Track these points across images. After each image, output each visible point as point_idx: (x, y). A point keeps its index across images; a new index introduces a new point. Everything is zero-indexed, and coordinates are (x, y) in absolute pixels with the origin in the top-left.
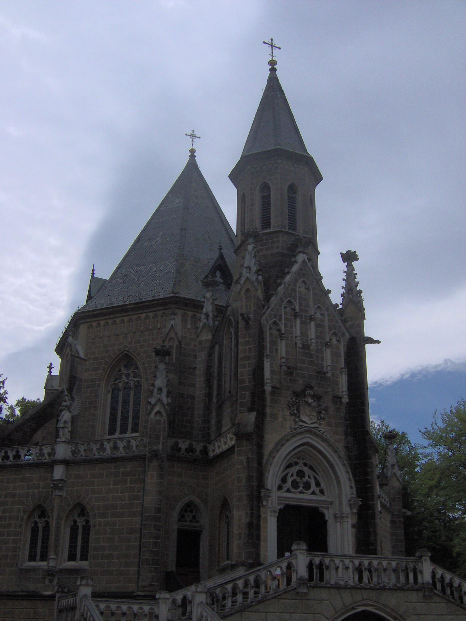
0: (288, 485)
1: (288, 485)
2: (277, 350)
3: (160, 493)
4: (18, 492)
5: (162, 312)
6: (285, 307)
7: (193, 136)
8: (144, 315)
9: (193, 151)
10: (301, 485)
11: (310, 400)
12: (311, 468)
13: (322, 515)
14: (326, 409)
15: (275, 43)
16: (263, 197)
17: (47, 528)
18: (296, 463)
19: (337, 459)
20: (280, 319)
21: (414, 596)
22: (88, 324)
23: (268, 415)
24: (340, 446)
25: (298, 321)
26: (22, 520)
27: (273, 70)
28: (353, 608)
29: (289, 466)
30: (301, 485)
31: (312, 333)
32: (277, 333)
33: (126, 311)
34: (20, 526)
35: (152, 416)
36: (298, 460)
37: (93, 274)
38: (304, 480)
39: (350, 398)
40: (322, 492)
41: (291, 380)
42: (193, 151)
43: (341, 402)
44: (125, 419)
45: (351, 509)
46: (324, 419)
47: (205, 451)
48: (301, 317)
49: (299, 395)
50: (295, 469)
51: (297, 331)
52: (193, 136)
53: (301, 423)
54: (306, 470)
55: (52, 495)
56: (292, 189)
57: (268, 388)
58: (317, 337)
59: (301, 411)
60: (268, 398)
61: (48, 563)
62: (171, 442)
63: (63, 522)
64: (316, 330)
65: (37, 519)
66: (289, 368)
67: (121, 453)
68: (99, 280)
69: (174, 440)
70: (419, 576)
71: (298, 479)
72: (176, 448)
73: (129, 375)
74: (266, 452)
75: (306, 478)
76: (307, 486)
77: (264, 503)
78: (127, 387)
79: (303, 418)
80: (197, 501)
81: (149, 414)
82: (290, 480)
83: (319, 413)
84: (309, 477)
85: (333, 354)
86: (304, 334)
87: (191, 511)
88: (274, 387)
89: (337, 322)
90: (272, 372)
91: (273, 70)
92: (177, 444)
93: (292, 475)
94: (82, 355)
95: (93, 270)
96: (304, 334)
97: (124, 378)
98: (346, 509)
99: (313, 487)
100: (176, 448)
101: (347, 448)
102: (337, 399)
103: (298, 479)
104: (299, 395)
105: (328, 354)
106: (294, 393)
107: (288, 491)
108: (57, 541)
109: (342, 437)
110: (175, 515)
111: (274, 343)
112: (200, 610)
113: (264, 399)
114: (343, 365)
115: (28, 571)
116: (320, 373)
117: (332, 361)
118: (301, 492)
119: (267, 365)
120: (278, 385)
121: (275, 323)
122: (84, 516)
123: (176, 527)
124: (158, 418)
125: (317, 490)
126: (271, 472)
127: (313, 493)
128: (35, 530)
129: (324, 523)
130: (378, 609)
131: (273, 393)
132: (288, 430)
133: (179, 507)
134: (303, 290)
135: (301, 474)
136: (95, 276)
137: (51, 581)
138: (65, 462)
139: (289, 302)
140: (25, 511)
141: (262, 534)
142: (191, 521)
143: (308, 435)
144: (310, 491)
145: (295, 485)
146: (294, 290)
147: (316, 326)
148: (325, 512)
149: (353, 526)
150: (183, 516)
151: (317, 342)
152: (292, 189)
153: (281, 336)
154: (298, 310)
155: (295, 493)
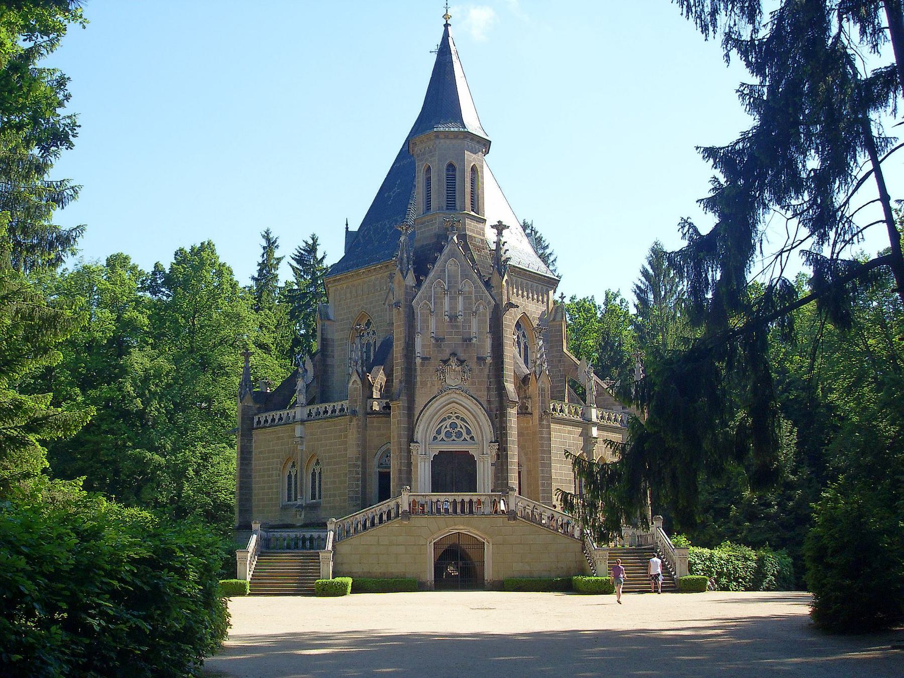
0: (443, 435)
1: (443, 435)
12: (463, 419)
18: (449, 417)
20: (430, 301)
24: (484, 400)
27: (447, 26)
29: (444, 420)
31: (460, 307)
34: (279, 476)
35: (351, 384)
36: (451, 415)
37: (347, 228)
40: (472, 438)
41: (438, 351)
43: (485, 364)
49: (445, 362)
51: (446, 307)
54: (456, 421)
56: (451, 167)
57: (418, 361)
60: (418, 368)
64: (465, 304)
66: (437, 340)
71: (451, 430)
74: (417, 413)
86: (453, 307)
88: (423, 359)
90: (423, 346)
91: (447, 26)
93: (446, 427)
94: (332, 317)
95: (347, 225)
96: (453, 307)
99: (465, 435)
101: (489, 402)
102: (481, 359)
104: (445, 362)
105: (474, 322)
110: (376, 462)
111: (425, 321)
113: (415, 369)
117: (479, 328)
119: (418, 340)
124: (355, 386)
126: (421, 427)
131: (422, 365)
138: (303, 422)
140: (281, 463)
144: (463, 438)
145: (448, 434)
152: (451, 167)
154: (446, 288)
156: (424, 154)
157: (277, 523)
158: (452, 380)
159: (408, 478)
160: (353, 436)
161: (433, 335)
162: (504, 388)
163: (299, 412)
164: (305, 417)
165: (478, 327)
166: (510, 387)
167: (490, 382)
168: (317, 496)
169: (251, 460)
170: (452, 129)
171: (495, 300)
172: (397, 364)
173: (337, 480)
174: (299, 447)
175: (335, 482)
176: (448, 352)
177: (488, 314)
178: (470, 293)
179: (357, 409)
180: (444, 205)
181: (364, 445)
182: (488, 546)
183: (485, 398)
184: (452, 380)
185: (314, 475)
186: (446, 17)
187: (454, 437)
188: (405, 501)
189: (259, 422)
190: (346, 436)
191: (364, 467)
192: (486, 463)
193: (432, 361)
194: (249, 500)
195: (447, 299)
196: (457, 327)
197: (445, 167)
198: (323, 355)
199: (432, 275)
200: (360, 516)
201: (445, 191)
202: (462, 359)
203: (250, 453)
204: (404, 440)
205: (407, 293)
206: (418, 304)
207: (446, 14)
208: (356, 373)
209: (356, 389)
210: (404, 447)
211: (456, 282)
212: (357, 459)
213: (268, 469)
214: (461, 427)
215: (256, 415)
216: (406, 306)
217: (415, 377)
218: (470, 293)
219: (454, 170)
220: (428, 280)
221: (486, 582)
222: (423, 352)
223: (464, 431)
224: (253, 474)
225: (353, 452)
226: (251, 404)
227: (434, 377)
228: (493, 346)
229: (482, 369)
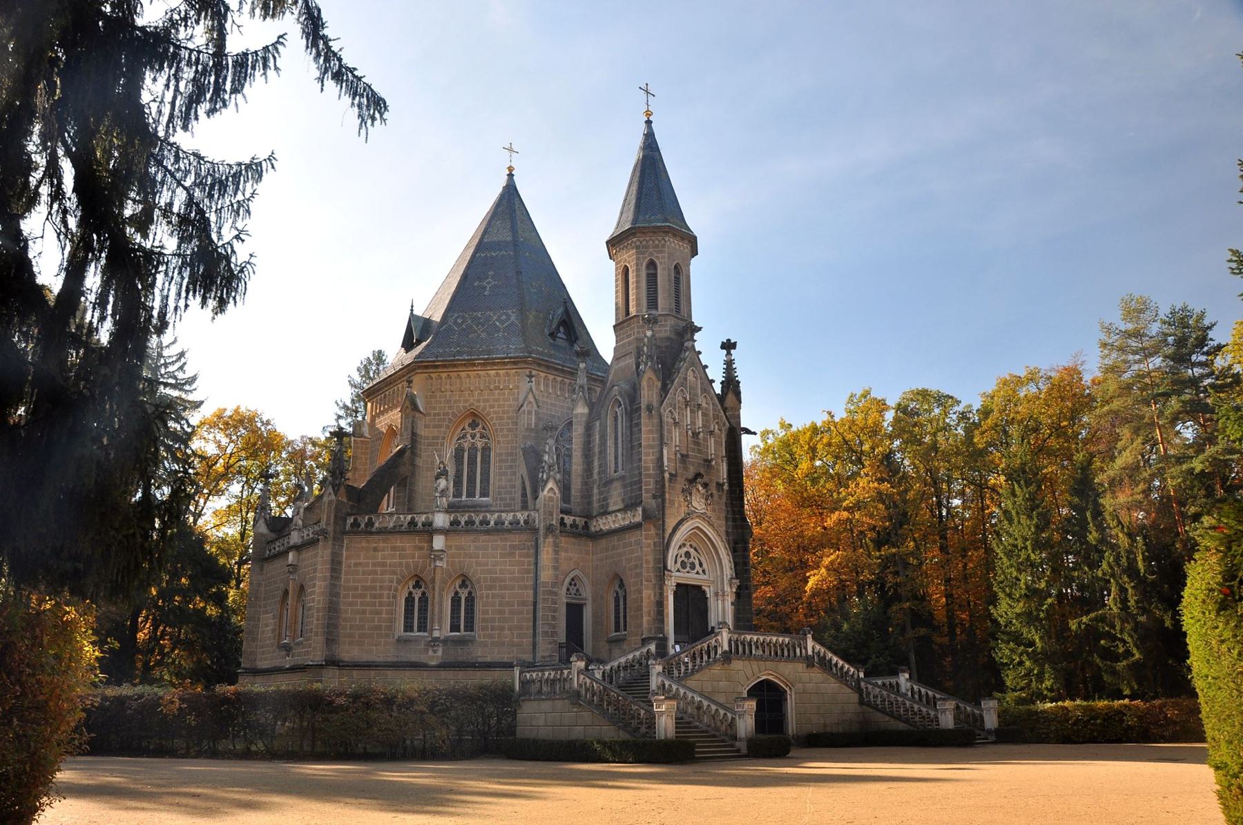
1: (679, 565)
2: (672, 438)
3: (556, 568)
4: (389, 561)
5: (514, 371)
7: (511, 150)
9: (511, 169)
10: (689, 565)
11: (701, 488)
12: (695, 549)
13: (704, 592)
16: (648, 275)
17: (424, 599)
18: (684, 545)
20: (675, 409)
22: (426, 375)
23: (667, 501)
26: (396, 590)
27: (649, 122)
31: (700, 423)
32: (672, 420)
34: (395, 597)
35: (545, 492)
37: (412, 310)
39: (730, 485)
40: (704, 571)
42: (511, 169)
43: (723, 490)
44: (472, 481)
45: (731, 587)
47: (586, 526)
48: (690, 406)
49: (692, 481)
50: (685, 549)
52: (511, 150)
54: (692, 551)
55: (430, 566)
56: (677, 269)
57: (667, 475)
59: (693, 498)
60: (667, 484)
61: (432, 634)
63: (444, 594)
64: (703, 421)
65: (411, 589)
66: (682, 455)
70: (804, 651)
71: (686, 560)
73: (475, 435)
74: (667, 536)
75: (692, 560)
78: (473, 449)
80: (581, 575)
82: (679, 560)
83: (706, 499)
87: (575, 585)
91: (649, 122)
94: (422, 410)
95: (412, 306)
96: (693, 423)
98: (727, 588)
101: (727, 532)
103: (686, 560)
104: (692, 481)
106: (687, 480)
108: (441, 612)
109: (724, 523)
111: (670, 432)
112: (660, 679)
115: (406, 641)
117: (715, 451)
118: (688, 572)
119: (665, 452)
120: (674, 472)
121: (670, 411)
122: (466, 587)
123: (565, 601)
124: (551, 494)
127: (698, 573)
128: (409, 600)
129: (704, 599)
131: (670, 480)
133: (568, 580)
135: (688, 554)
136: (415, 313)
137: (435, 652)
139: (682, 390)
140: (399, 582)
142: (575, 594)
143: (697, 520)
144: (695, 571)
145: (683, 565)
146: (685, 379)
147: (704, 414)
148: (707, 589)
149: (732, 604)
150: (568, 589)
153: (676, 424)
155: (684, 573)
158: (698, 504)
164: (447, 525)
167: (728, 511)
169: (340, 573)
171: (729, 422)
172: (649, 476)
173: (507, 609)
174: (438, 563)
179: (554, 522)
183: (724, 528)
185: (456, 601)
186: (648, 113)
187: (688, 569)
189: (356, 524)
193: (678, 478)
194: (336, 626)
196: (697, 444)
203: (340, 563)
207: (648, 111)
209: (551, 499)
213: (374, 588)
215: (350, 515)
218: (706, 409)
223: (697, 562)
224: (343, 592)
226: (345, 500)
229: (720, 495)
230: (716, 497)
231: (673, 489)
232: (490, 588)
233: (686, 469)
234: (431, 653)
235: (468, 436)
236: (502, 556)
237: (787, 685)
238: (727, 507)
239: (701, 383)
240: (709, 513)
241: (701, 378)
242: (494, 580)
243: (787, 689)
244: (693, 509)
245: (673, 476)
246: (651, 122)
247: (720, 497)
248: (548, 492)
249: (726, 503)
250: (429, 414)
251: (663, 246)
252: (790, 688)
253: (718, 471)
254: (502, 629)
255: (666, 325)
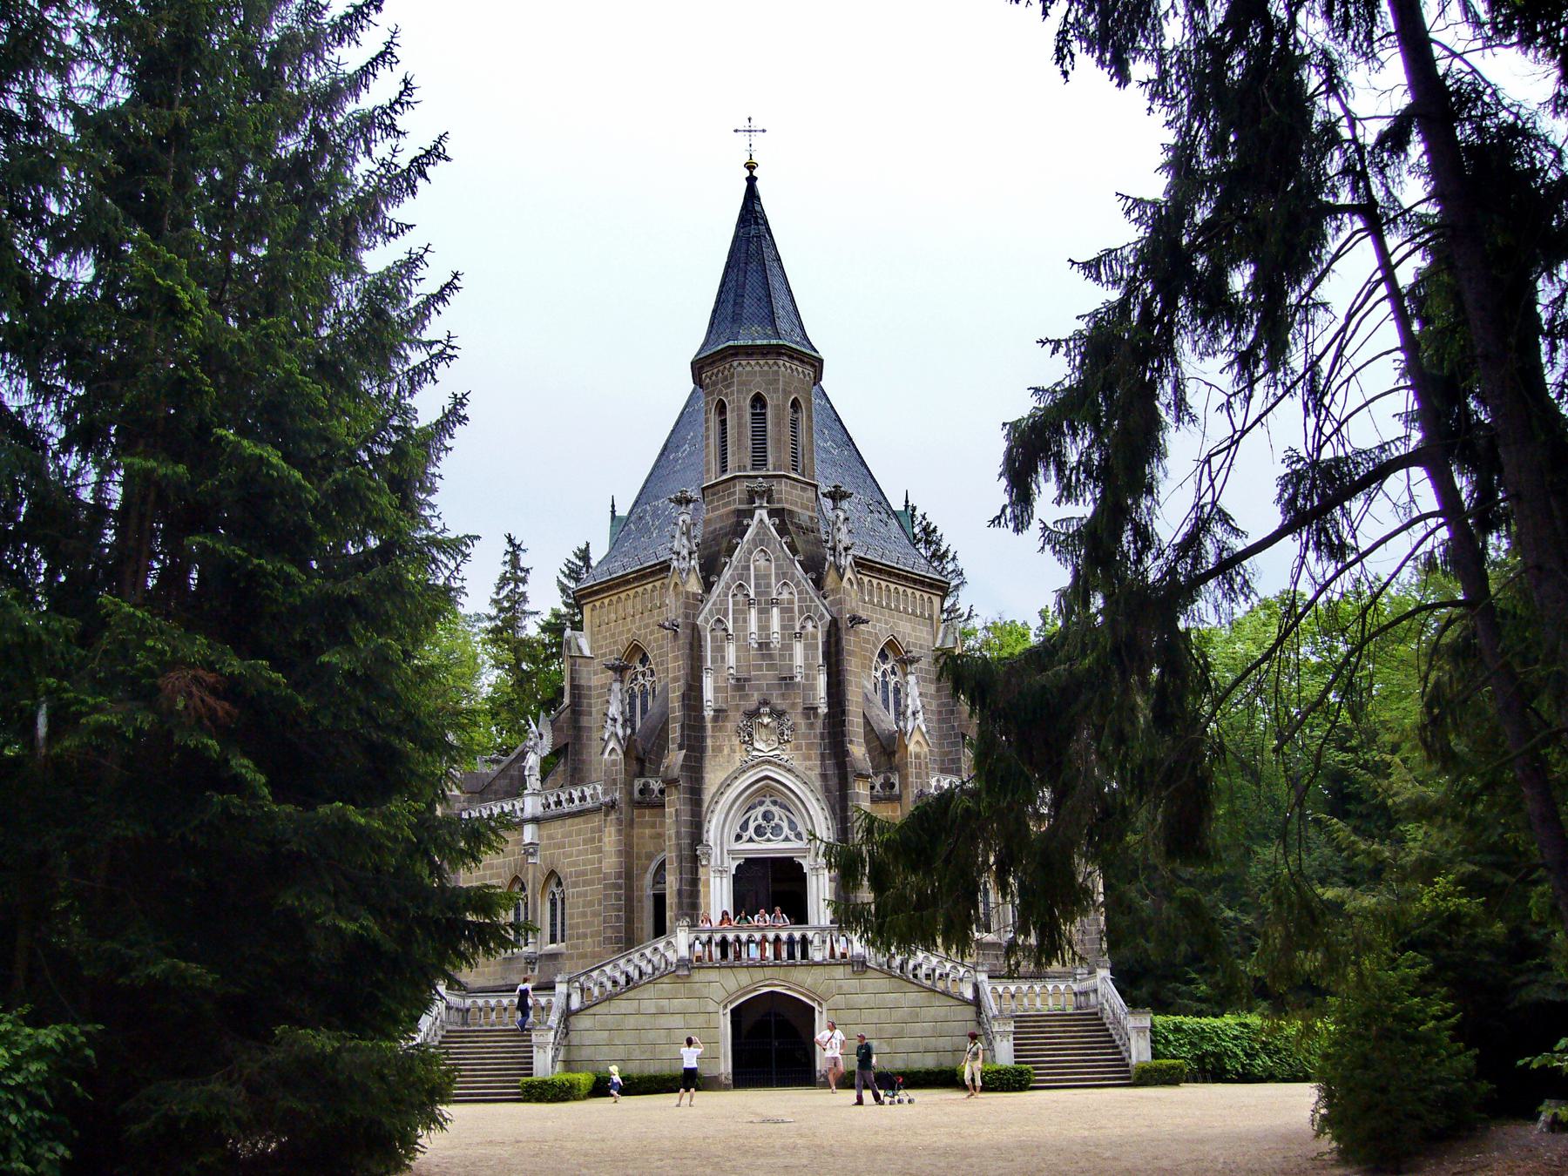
2: (723, 658)
6: (734, 595)
8: (650, 586)
10: (769, 831)
11: (766, 720)
13: (800, 866)
14: (793, 729)
15: (755, 124)
18: (761, 803)
19: (809, 794)
21: (839, 972)
24: (814, 774)
25: (753, 611)
27: (751, 180)
28: (755, 990)
30: (769, 831)
33: (628, 582)
35: (606, 755)
37: (613, 512)
38: (773, 824)
39: (829, 705)
43: (816, 715)
46: (788, 741)
49: (753, 714)
51: (753, 626)
53: (755, 753)
54: (774, 809)
57: (708, 713)
58: (783, 627)
59: (756, 737)
60: (709, 725)
62: (638, 784)
64: (782, 619)
67: (589, 803)
68: (621, 518)
69: (643, 780)
71: (764, 823)
72: (645, 790)
74: (707, 797)
75: (776, 820)
76: (777, 830)
77: (704, 863)
79: (757, 745)
81: (602, 753)
82: (752, 826)
84: (781, 819)
85: (806, 647)
86: (764, 627)
88: (715, 711)
89: (812, 600)
90: (716, 690)
91: (751, 180)
92: (646, 785)
93: (756, 819)
94: (587, 652)
95: (613, 506)
96: (764, 627)
97: (640, 677)
99: (786, 830)
100: (645, 790)
101: (824, 776)
102: (811, 710)
104: (753, 714)
105: (798, 649)
107: (751, 840)
110: (648, 878)
111: (719, 650)
113: (703, 728)
114: (821, 662)
116: (785, 678)
117: (806, 658)
118: (769, 840)
119: (708, 684)
124: (614, 757)
125: (792, 836)
126: (714, 822)
127: (787, 839)
130: (789, 989)
131: (715, 719)
132: (738, 764)
133: (653, 866)
134: (762, 563)
135: (767, 816)
138: (535, 820)
141: (702, 901)
145: (759, 831)
147: (783, 611)
148: (801, 861)
151: (783, 636)
154: (752, 595)
156: (715, 384)
157: (491, 984)
158: (763, 745)
159: (691, 905)
160: (610, 838)
161: (732, 671)
162: (846, 753)
163: (530, 805)
165: (803, 659)
166: (858, 751)
168: (559, 937)
170: (759, 342)
173: (588, 910)
175: (584, 915)
176: (756, 697)
177: (820, 635)
178: (791, 602)
179: (617, 795)
180: (748, 462)
181: (628, 852)
182: (821, 1013)
183: (818, 771)
184: (763, 745)
187: (769, 835)
188: (681, 941)
190: (600, 840)
191: (629, 888)
192: (821, 877)
195: (753, 612)
196: (771, 657)
197: (748, 401)
198: (574, 712)
199: (727, 573)
200: (614, 971)
201: (750, 442)
202: (779, 708)
204: (686, 841)
205: (687, 606)
206: (707, 621)
208: (613, 739)
209: (614, 763)
210: (686, 853)
211: (768, 585)
212: (619, 876)
214: (781, 819)
216: (686, 625)
217: (703, 739)
219: (764, 406)
220: (722, 584)
221: (818, 1074)
222: (716, 699)
223: (785, 825)
225: (610, 863)
227: (733, 738)
228: (829, 685)
229: (812, 724)
230: (803, 729)
231: (721, 729)
232: (575, 885)
233: (744, 697)
234: (529, 972)
235: (640, 677)
236: (585, 842)
237: (814, 1000)
238: (822, 736)
239: (777, 567)
240: (785, 755)
241: (777, 559)
242: (578, 874)
243: (815, 1005)
244: (755, 753)
245: (719, 713)
246: (756, 178)
247: (811, 726)
248: (610, 753)
249: (822, 734)
250: (597, 656)
251: (732, 376)
252: (820, 1004)
253: (813, 688)
254: (585, 936)
255: (734, 493)
